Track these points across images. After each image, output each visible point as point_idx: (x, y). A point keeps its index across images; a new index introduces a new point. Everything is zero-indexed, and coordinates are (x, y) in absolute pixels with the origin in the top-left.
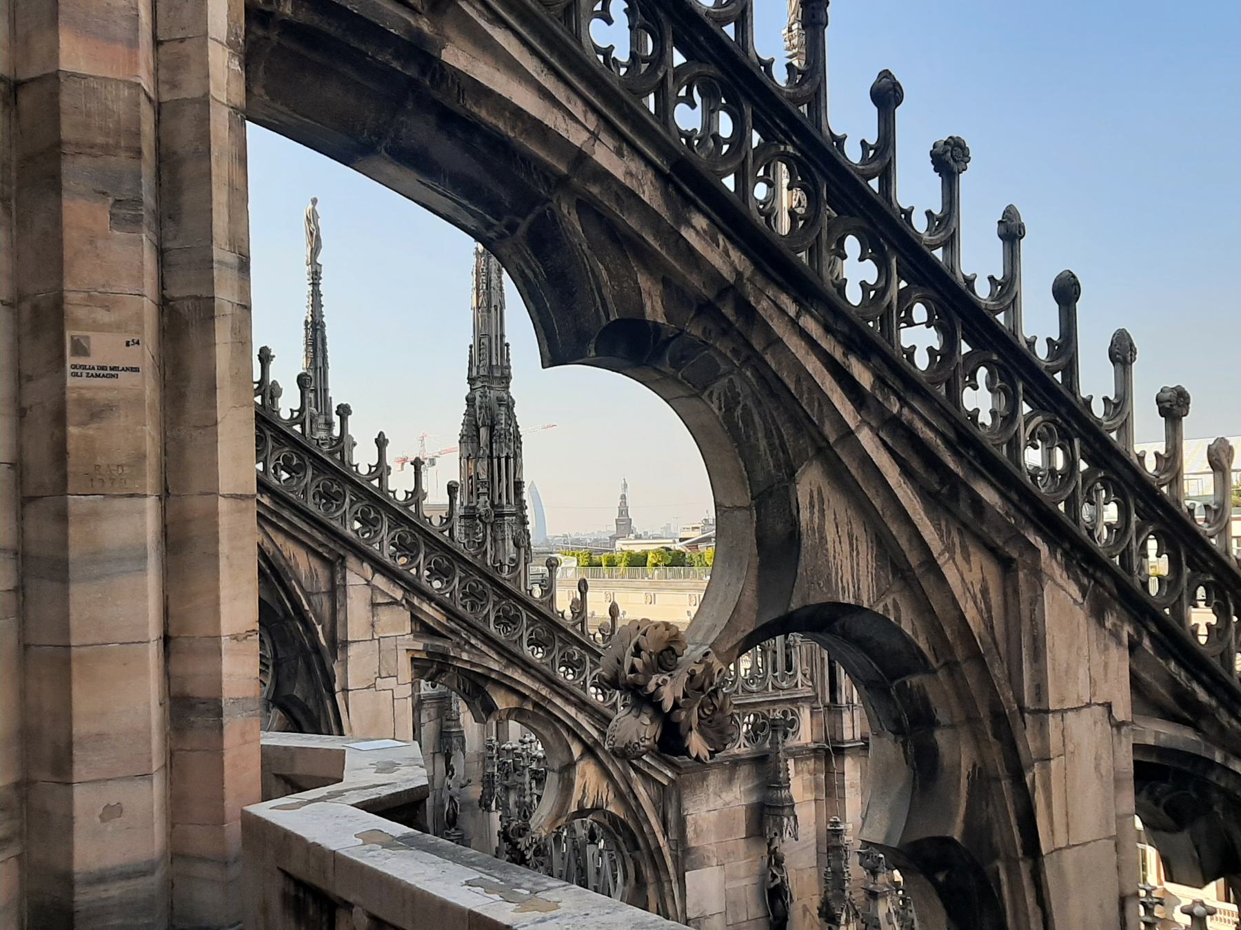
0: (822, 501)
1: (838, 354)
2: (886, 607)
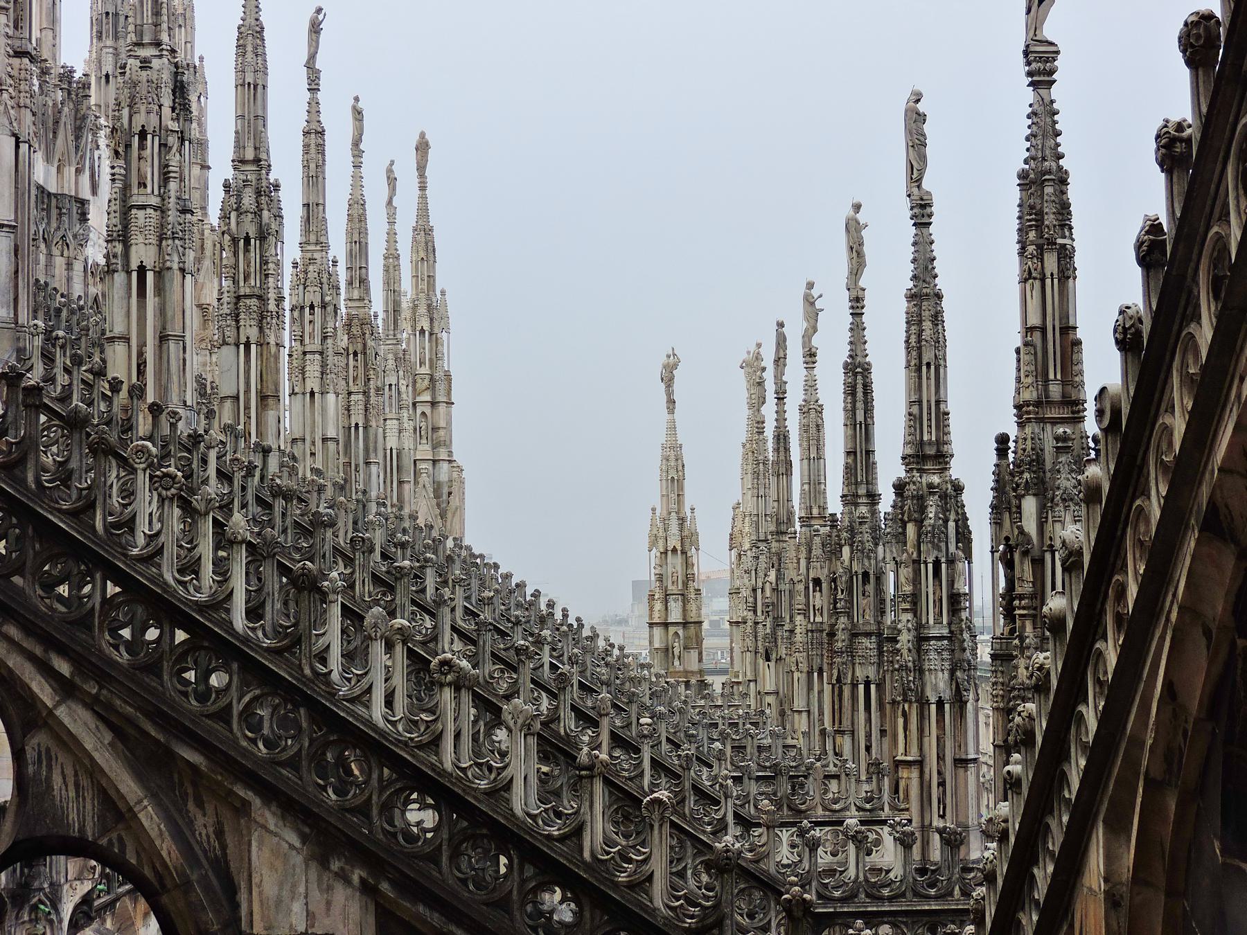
0: (49, 759)
1: (38, 651)
2: (110, 841)
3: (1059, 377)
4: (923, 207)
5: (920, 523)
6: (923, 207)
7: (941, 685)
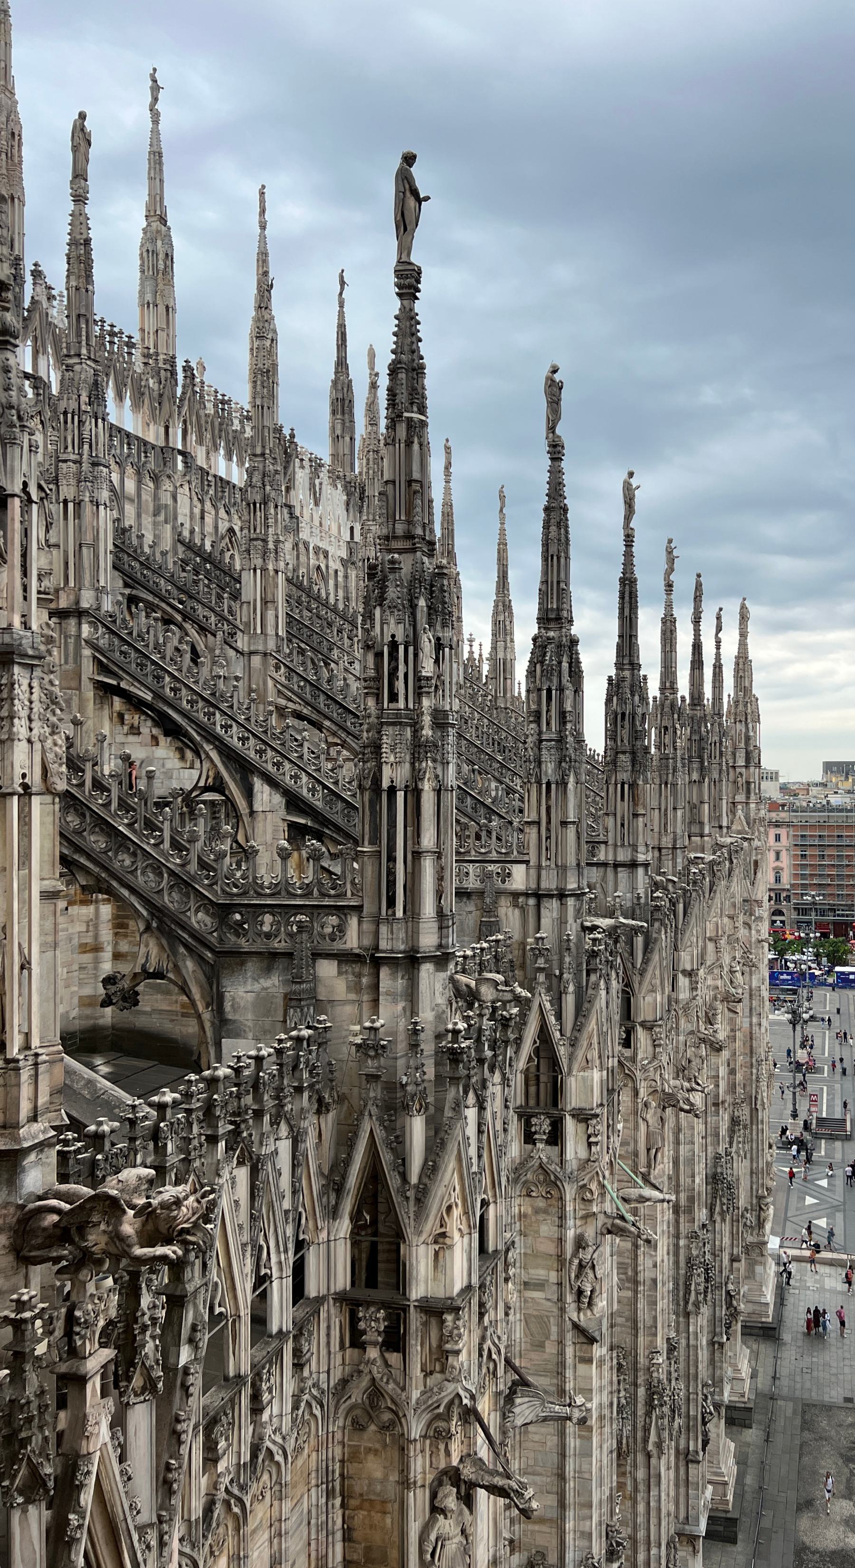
3: (403, 518)
4: (555, 446)
5: (542, 663)
6: (555, 446)
7: (550, 771)
